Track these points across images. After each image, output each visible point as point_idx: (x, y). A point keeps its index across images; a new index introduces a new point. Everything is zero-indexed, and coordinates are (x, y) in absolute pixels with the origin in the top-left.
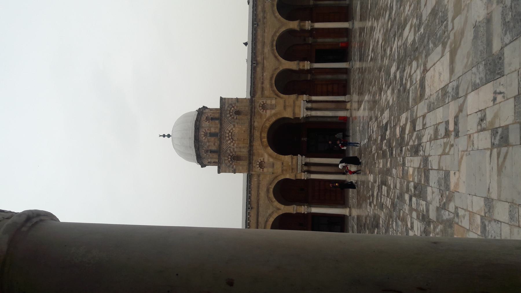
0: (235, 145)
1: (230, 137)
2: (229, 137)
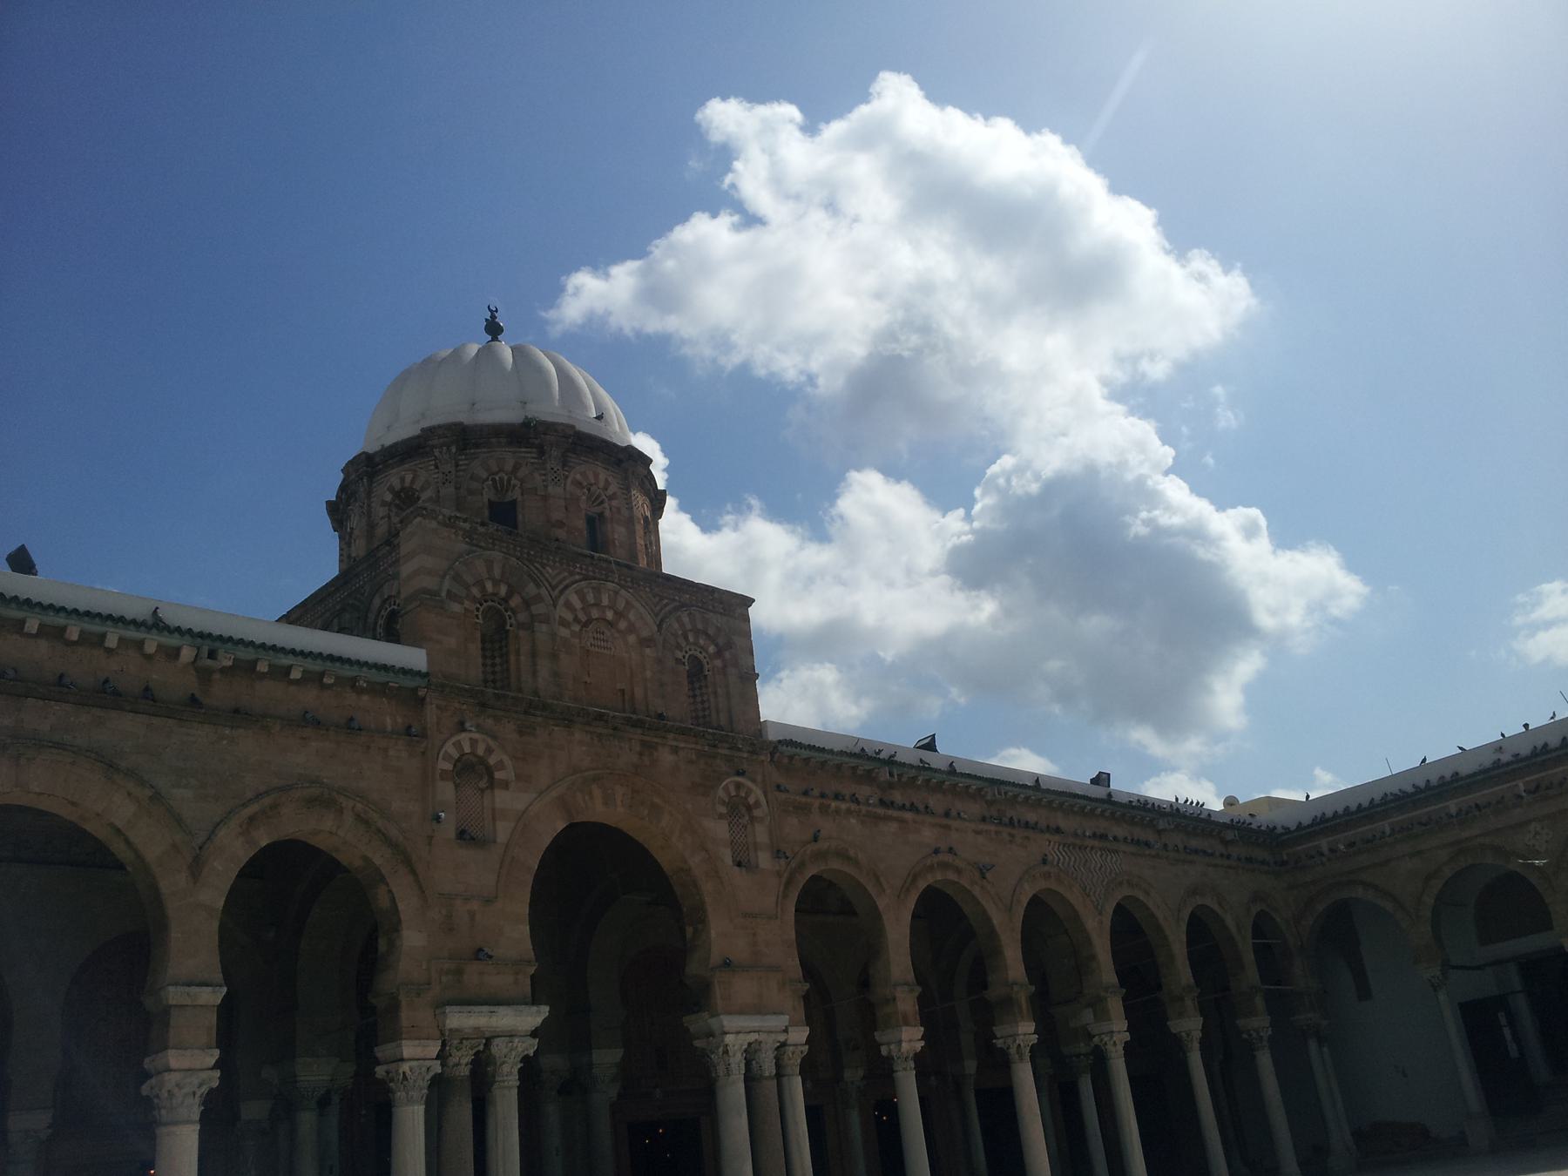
0: (564, 632)
1: (595, 614)
2: (597, 605)
